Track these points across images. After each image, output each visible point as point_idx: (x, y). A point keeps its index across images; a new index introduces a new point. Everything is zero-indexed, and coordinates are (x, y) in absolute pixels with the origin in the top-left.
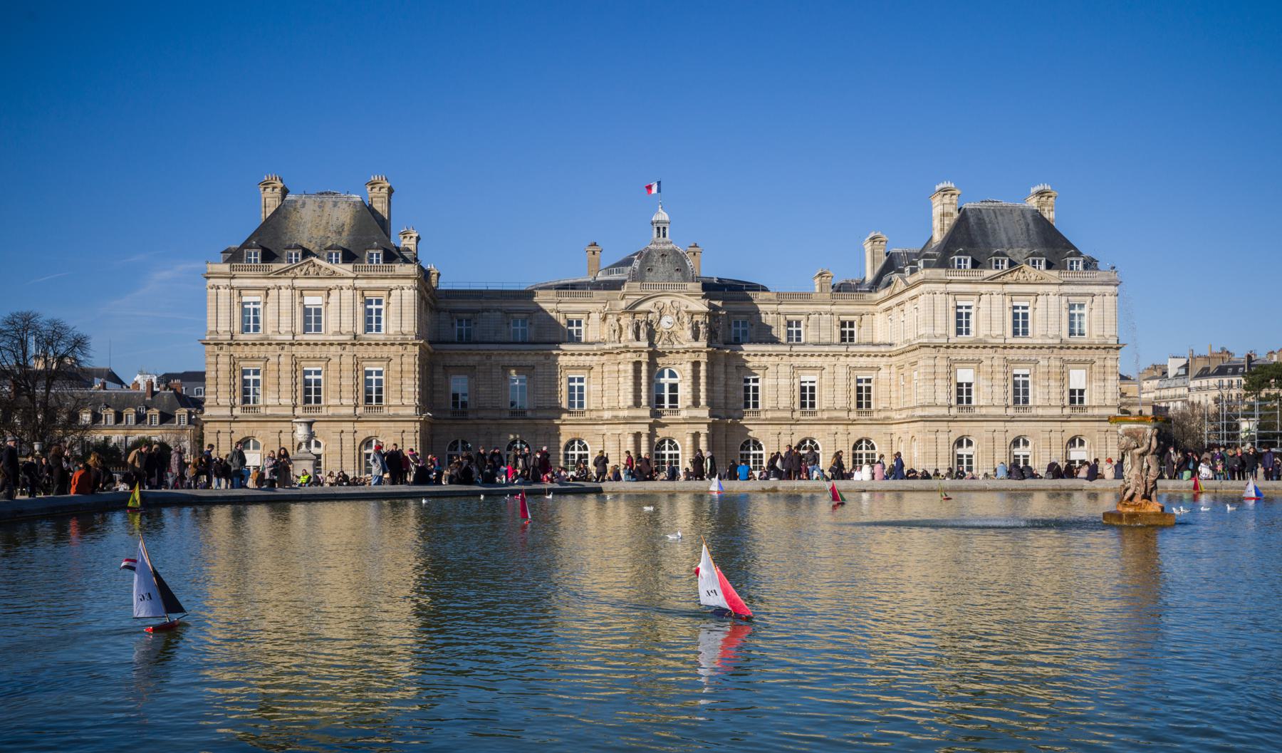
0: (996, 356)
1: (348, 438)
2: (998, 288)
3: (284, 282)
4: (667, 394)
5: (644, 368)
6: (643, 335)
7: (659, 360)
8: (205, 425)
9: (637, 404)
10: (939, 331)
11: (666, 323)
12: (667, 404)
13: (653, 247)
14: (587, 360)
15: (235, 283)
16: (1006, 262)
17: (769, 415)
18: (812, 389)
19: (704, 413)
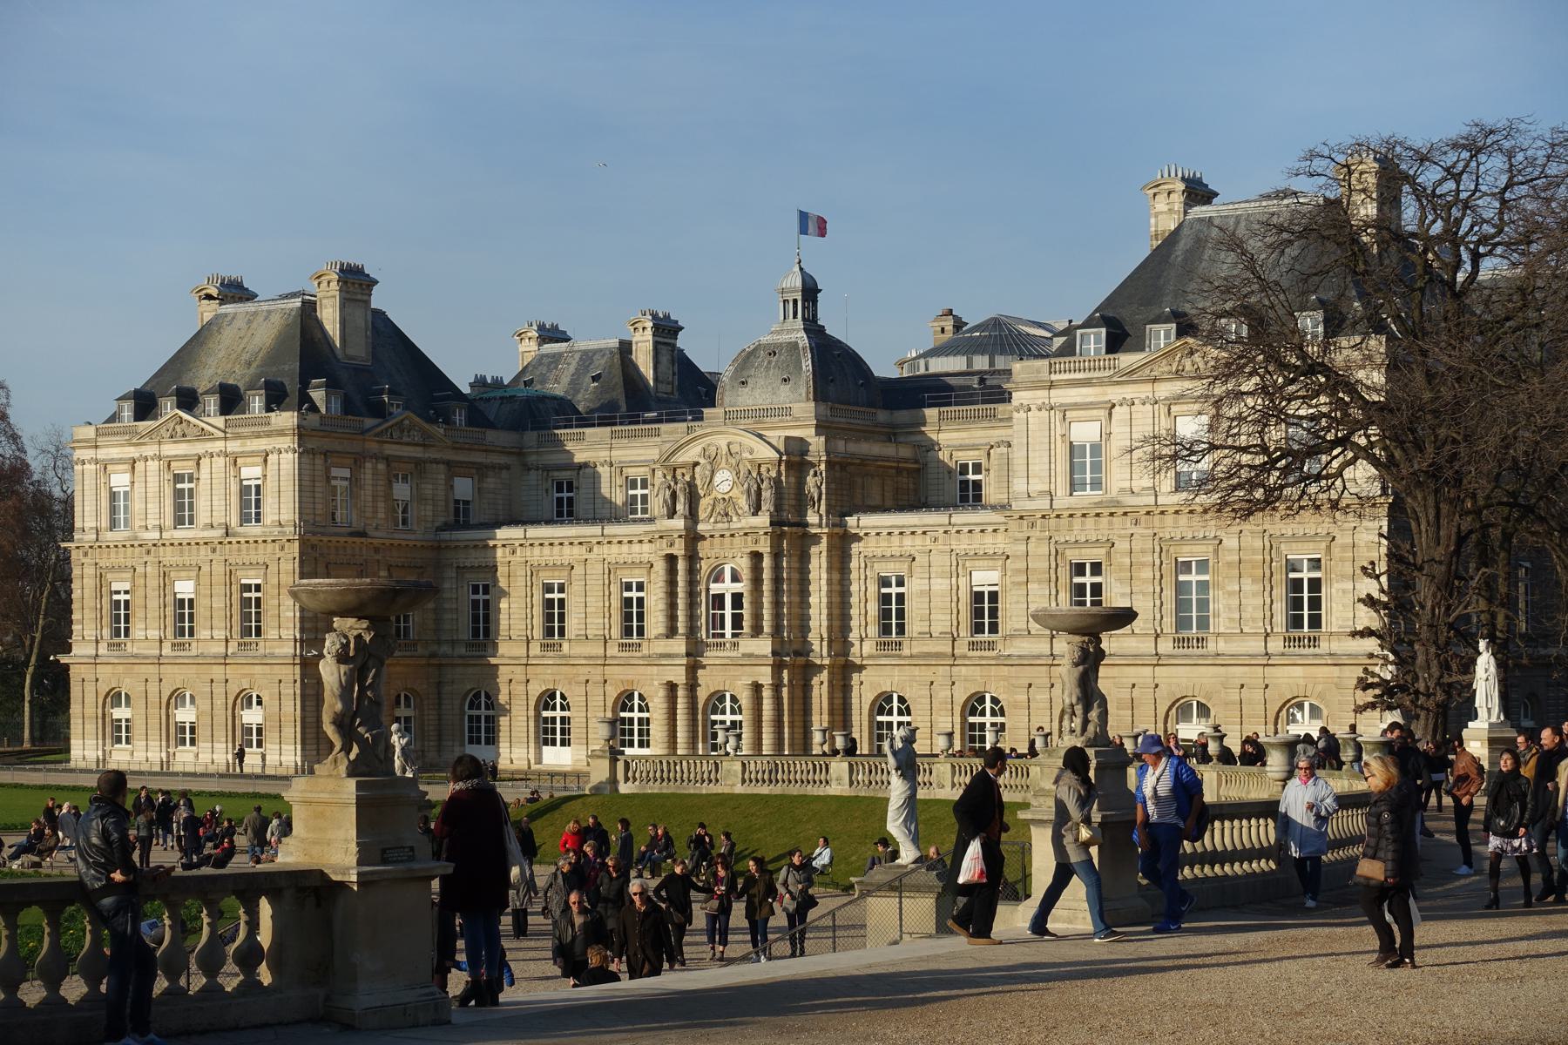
0: (1137, 530)
1: (219, 690)
2: (1144, 390)
3: (150, 450)
4: (728, 612)
5: (681, 566)
6: (680, 507)
7: (703, 548)
8: (73, 671)
9: (672, 632)
10: (1038, 486)
11: (724, 481)
12: (728, 631)
13: (766, 339)
14: (646, 552)
15: (102, 454)
16: (1173, 332)
17: (917, 648)
18: (994, 596)
19: (764, 646)
